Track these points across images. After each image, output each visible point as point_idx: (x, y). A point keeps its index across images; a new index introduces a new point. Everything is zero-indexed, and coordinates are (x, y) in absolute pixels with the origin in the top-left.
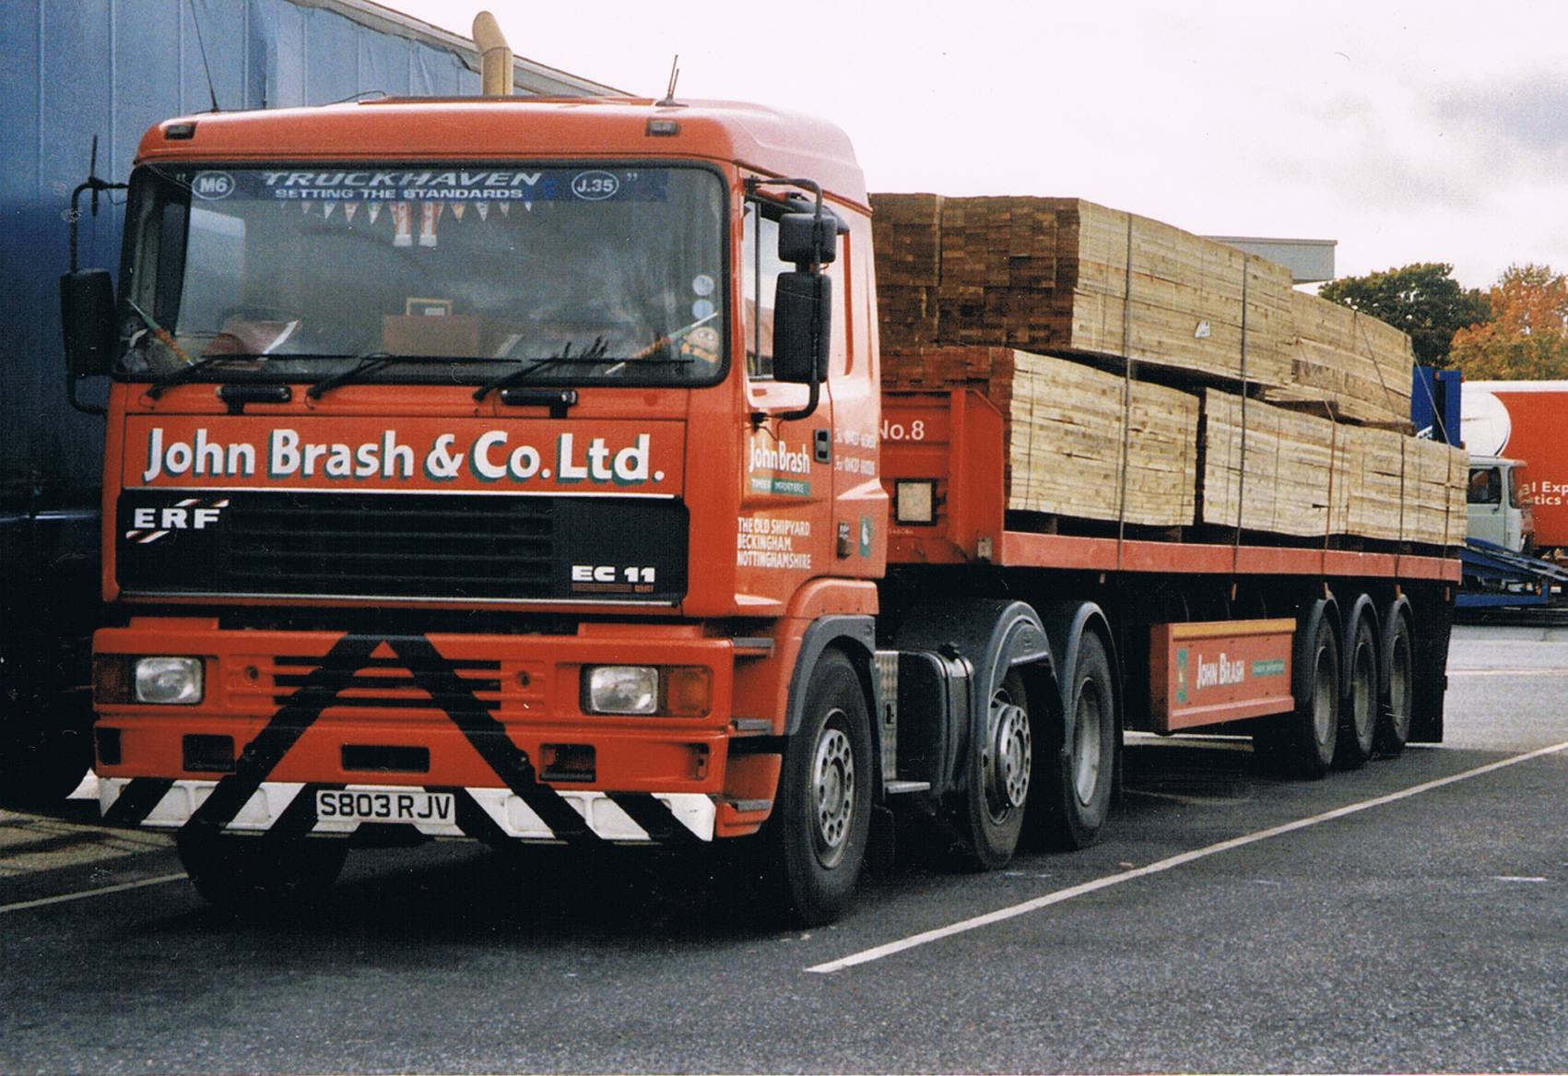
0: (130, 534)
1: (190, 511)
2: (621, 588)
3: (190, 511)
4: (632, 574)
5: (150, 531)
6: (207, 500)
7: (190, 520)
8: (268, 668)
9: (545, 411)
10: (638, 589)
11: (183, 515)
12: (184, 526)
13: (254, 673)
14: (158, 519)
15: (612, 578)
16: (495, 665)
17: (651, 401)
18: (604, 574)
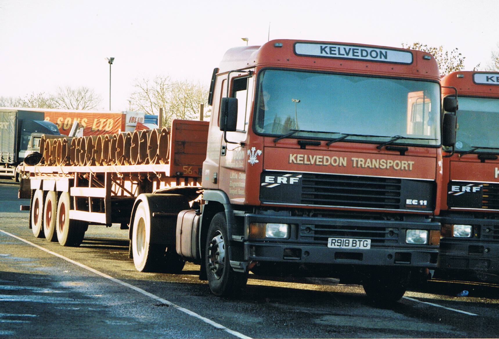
0: (263, 184)
1: (288, 178)
2: (420, 207)
3: (288, 178)
4: (421, 202)
5: (272, 184)
6: (294, 175)
7: (288, 181)
10: (423, 207)
11: (286, 179)
14: (276, 180)
15: (416, 203)
16: (384, 229)
18: (415, 202)
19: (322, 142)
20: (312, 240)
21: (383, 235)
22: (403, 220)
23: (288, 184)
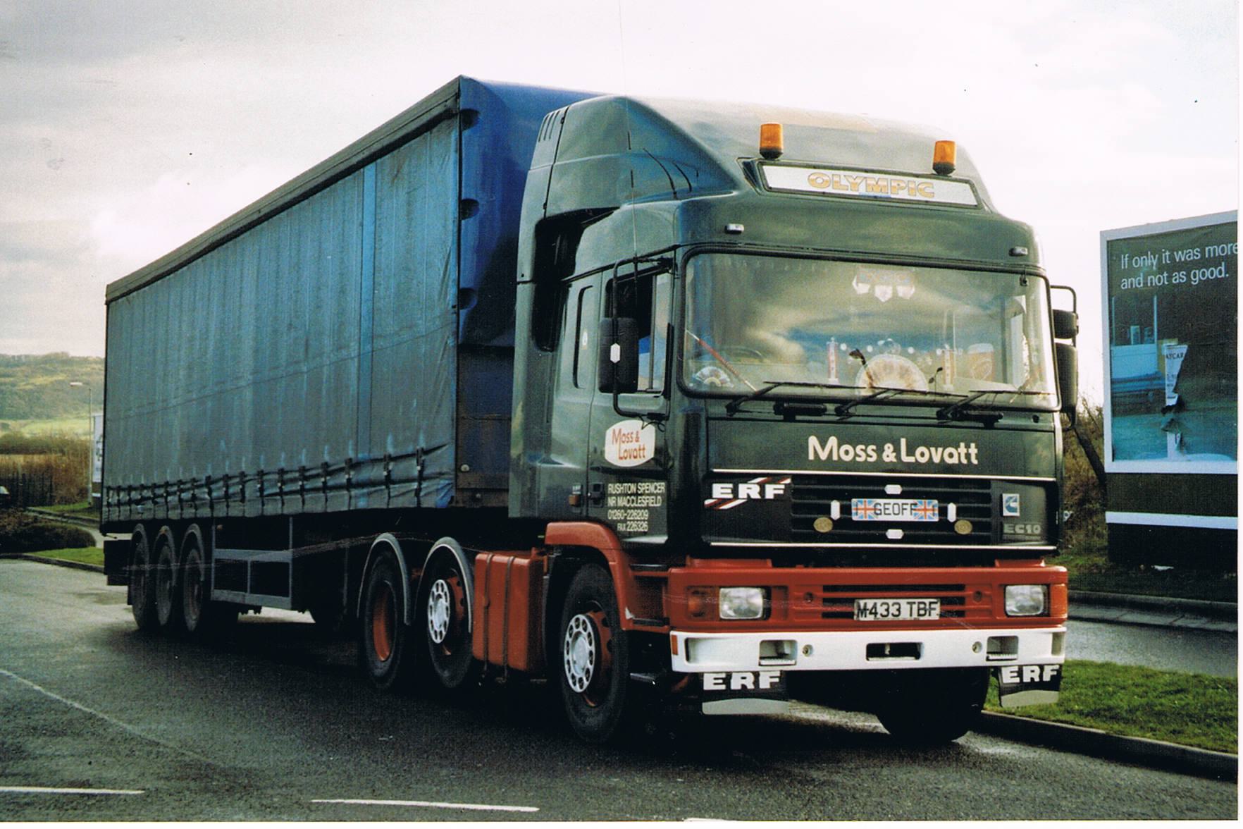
0: (708, 502)
1: (762, 486)
5: (729, 500)
6: (775, 479)
7: (762, 492)
8: (821, 594)
9: (981, 425)
11: (757, 488)
12: (758, 497)
13: (811, 596)
14: (735, 492)
16: (960, 587)
17: (1036, 420)
19: (831, 407)
20: (820, 620)
21: (961, 601)
22: (993, 565)
23: (763, 500)
